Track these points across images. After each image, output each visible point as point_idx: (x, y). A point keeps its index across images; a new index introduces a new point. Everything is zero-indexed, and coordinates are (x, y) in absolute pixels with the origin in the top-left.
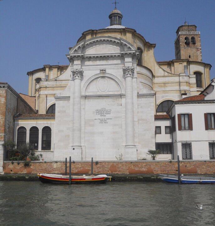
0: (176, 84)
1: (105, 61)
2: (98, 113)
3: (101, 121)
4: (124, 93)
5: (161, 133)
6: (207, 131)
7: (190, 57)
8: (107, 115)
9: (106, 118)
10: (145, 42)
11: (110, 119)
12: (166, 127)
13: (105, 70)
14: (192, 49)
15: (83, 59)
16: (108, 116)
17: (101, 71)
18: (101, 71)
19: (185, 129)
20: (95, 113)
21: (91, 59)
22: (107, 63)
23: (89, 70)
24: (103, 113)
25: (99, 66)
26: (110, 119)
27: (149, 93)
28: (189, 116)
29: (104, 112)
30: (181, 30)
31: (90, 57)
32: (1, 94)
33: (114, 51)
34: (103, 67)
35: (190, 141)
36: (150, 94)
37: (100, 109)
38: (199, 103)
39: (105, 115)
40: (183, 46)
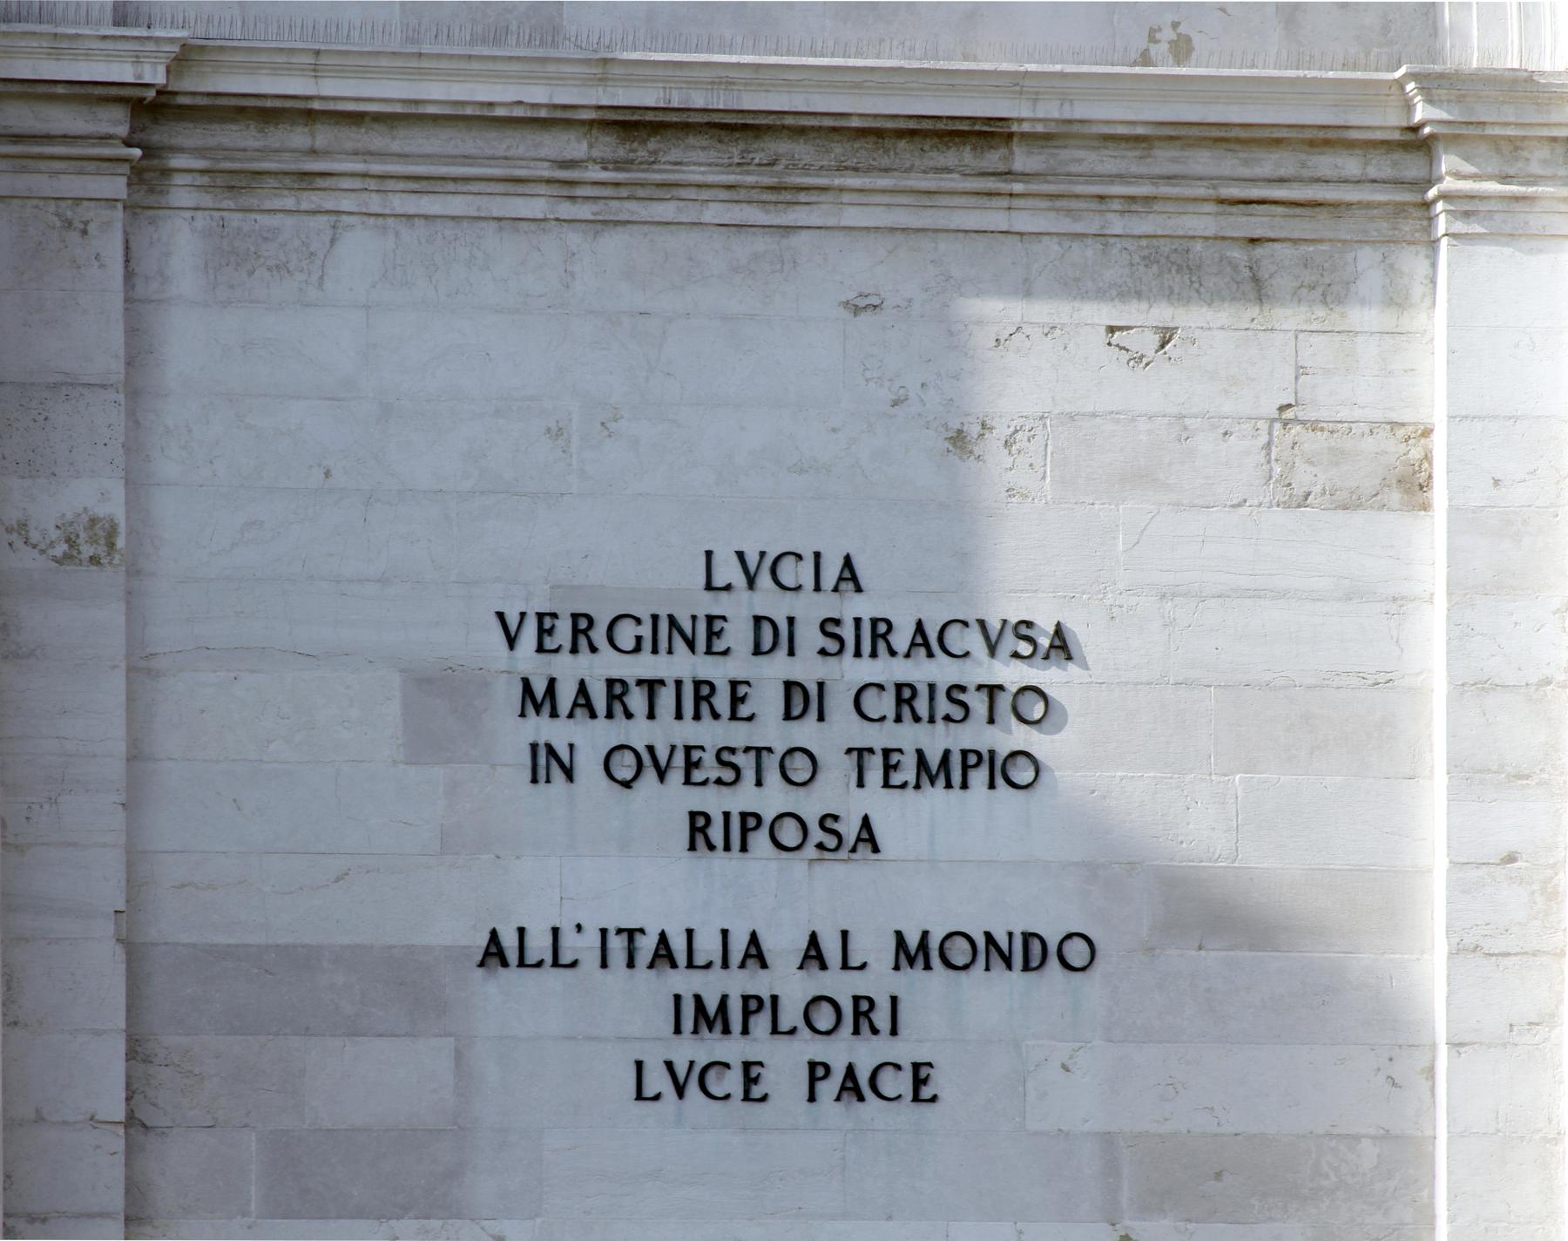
3: (710, 1018)
24: (772, 731)
37: (694, 604)
39: (875, 802)
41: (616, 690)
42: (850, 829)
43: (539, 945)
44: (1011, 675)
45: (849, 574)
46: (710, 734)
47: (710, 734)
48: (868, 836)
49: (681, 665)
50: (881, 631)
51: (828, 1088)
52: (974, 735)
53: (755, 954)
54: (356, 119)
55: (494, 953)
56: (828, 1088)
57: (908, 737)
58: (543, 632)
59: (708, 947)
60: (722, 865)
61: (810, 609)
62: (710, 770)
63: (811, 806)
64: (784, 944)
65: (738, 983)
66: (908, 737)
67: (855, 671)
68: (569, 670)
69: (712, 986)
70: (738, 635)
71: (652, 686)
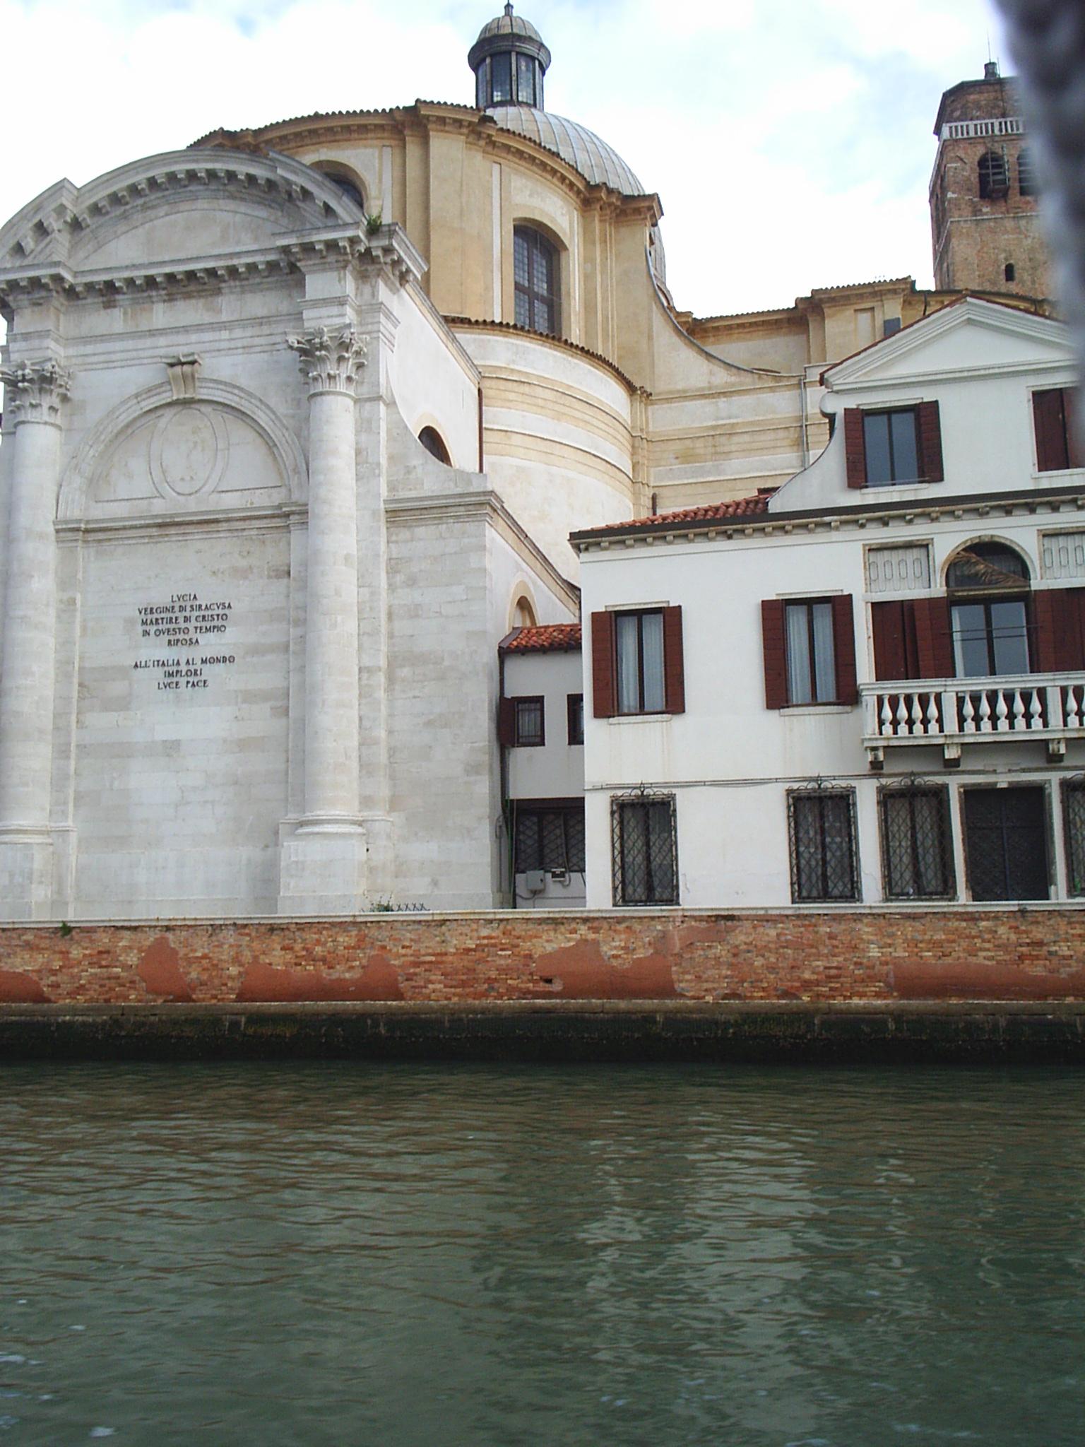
0: (782, 434)
2: (153, 629)
3: (171, 675)
5: (543, 744)
6: (774, 714)
7: (1010, 273)
8: (203, 638)
9: (197, 653)
10: (581, 186)
13: (193, 363)
14: (1023, 222)
16: (211, 644)
17: (172, 365)
18: (172, 365)
19: (642, 711)
20: (140, 629)
21: (119, 297)
22: (207, 318)
23: (109, 365)
24: (183, 625)
27: (459, 490)
28: (671, 618)
29: (186, 619)
30: (957, 114)
31: (110, 286)
34: (181, 346)
35: (666, 785)
36: (461, 495)
38: (730, 537)
39: (198, 636)
40: (967, 211)
41: (157, 619)
42: (194, 641)
43: (143, 664)
44: (221, 612)
45: (195, 597)
46: (171, 626)
47: (171, 626)
48: (197, 641)
49: (168, 615)
50: (200, 606)
51: (190, 685)
52: (215, 623)
53: (178, 663)
54: (116, 529)
55: (136, 666)
56: (190, 685)
57: (204, 624)
58: (146, 610)
59: (171, 662)
60: (174, 648)
61: (189, 604)
62: (172, 632)
63: (187, 637)
64: (183, 662)
65: (175, 668)
66: (204, 624)
67: (196, 613)
68: (149, 617)
69: (171, 669)
70: (177, 609)
71: (162, 619)
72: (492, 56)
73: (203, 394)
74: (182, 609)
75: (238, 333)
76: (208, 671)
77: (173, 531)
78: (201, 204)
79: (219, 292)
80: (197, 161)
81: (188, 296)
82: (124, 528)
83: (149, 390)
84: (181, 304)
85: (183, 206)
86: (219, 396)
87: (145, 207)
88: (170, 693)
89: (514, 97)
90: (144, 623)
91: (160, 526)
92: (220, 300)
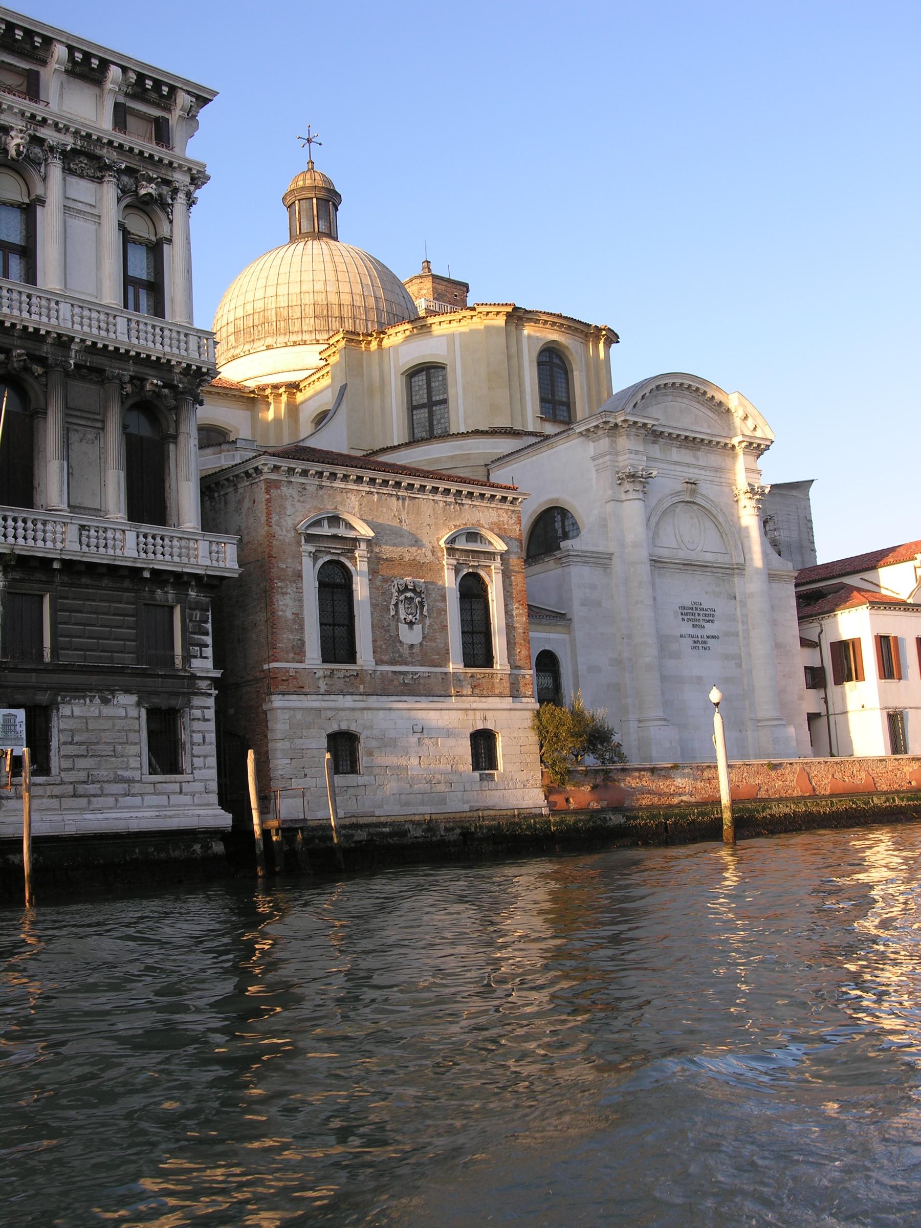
1: (690, 453)
2: (686, 618)
3: (695, 642)
4: (743, 562)
8: (707, 625)
11: (714, 637)
12: (806, 668)
15: (655, 435)
16: (710, 629)
21: (661, 440)
22: (693, 461)
24: (697, 618)
25: (678, 468)
26: (714, 637)
32: (506, 526)
33: (709, 427)
46: (693, 617)
47: (693, 617)
49: (690, 611)
64: (700, 636)
67: (702, 612)
68: (683, 611)
72: (317, 199)
73: (698, 500)
74: (696, 609)
75: (708, 473)
76: (711, 642)
77: (688, 567)
78: (685, 401)
79: (699, 449)
80: (694, 382)
81: (687, 448)
82: (671, 563)
83: (676, 493)
84: (683, 451)
85: (679, 400)
86: (703, 503)
87: (664, 395)
88: (695, 652)
89: (316, 230)
90: (682, 614)
91: (684, 564)
92: (699, 453)
